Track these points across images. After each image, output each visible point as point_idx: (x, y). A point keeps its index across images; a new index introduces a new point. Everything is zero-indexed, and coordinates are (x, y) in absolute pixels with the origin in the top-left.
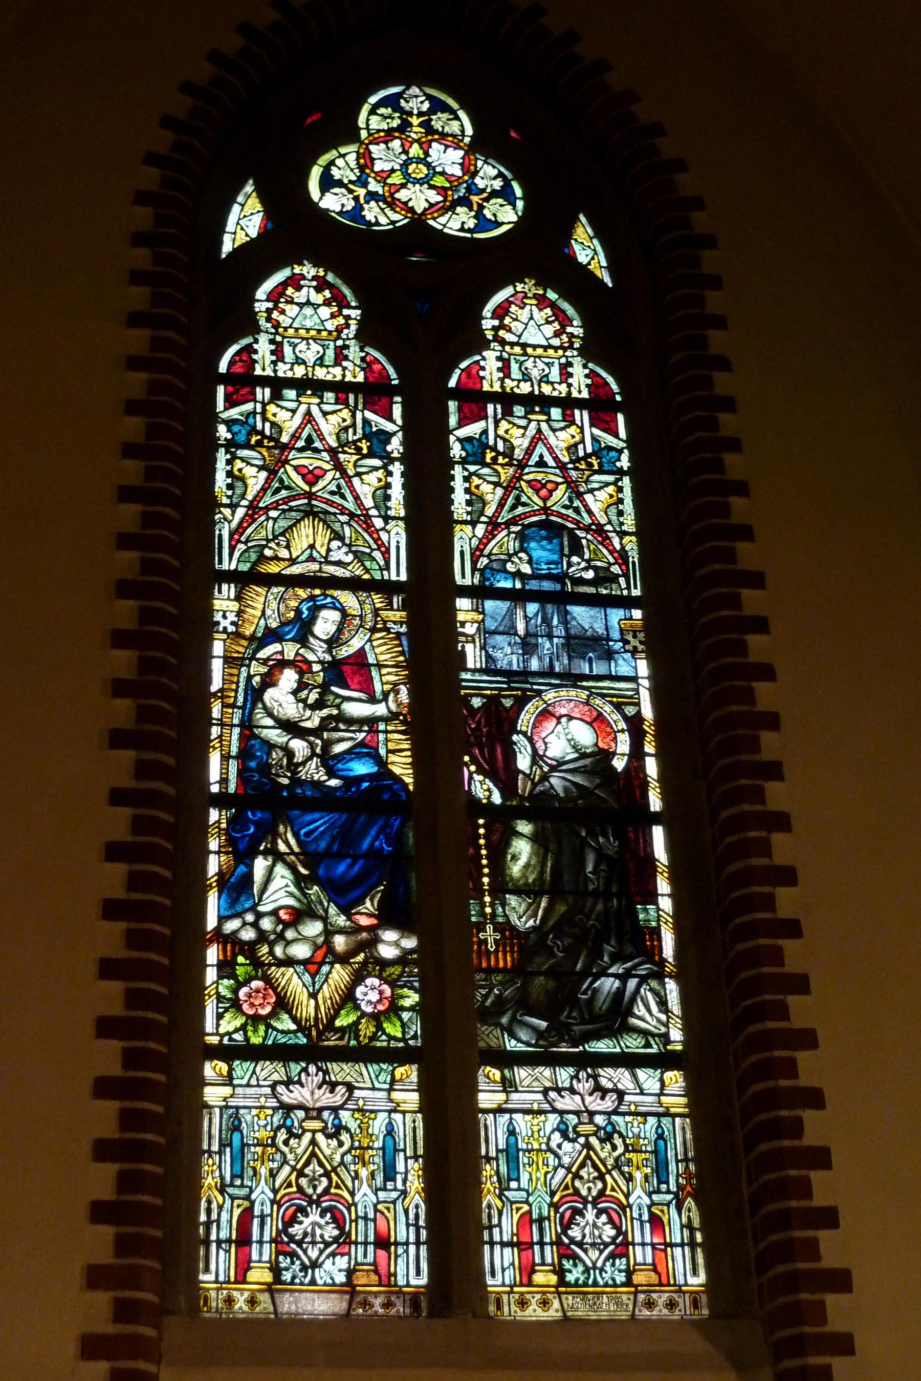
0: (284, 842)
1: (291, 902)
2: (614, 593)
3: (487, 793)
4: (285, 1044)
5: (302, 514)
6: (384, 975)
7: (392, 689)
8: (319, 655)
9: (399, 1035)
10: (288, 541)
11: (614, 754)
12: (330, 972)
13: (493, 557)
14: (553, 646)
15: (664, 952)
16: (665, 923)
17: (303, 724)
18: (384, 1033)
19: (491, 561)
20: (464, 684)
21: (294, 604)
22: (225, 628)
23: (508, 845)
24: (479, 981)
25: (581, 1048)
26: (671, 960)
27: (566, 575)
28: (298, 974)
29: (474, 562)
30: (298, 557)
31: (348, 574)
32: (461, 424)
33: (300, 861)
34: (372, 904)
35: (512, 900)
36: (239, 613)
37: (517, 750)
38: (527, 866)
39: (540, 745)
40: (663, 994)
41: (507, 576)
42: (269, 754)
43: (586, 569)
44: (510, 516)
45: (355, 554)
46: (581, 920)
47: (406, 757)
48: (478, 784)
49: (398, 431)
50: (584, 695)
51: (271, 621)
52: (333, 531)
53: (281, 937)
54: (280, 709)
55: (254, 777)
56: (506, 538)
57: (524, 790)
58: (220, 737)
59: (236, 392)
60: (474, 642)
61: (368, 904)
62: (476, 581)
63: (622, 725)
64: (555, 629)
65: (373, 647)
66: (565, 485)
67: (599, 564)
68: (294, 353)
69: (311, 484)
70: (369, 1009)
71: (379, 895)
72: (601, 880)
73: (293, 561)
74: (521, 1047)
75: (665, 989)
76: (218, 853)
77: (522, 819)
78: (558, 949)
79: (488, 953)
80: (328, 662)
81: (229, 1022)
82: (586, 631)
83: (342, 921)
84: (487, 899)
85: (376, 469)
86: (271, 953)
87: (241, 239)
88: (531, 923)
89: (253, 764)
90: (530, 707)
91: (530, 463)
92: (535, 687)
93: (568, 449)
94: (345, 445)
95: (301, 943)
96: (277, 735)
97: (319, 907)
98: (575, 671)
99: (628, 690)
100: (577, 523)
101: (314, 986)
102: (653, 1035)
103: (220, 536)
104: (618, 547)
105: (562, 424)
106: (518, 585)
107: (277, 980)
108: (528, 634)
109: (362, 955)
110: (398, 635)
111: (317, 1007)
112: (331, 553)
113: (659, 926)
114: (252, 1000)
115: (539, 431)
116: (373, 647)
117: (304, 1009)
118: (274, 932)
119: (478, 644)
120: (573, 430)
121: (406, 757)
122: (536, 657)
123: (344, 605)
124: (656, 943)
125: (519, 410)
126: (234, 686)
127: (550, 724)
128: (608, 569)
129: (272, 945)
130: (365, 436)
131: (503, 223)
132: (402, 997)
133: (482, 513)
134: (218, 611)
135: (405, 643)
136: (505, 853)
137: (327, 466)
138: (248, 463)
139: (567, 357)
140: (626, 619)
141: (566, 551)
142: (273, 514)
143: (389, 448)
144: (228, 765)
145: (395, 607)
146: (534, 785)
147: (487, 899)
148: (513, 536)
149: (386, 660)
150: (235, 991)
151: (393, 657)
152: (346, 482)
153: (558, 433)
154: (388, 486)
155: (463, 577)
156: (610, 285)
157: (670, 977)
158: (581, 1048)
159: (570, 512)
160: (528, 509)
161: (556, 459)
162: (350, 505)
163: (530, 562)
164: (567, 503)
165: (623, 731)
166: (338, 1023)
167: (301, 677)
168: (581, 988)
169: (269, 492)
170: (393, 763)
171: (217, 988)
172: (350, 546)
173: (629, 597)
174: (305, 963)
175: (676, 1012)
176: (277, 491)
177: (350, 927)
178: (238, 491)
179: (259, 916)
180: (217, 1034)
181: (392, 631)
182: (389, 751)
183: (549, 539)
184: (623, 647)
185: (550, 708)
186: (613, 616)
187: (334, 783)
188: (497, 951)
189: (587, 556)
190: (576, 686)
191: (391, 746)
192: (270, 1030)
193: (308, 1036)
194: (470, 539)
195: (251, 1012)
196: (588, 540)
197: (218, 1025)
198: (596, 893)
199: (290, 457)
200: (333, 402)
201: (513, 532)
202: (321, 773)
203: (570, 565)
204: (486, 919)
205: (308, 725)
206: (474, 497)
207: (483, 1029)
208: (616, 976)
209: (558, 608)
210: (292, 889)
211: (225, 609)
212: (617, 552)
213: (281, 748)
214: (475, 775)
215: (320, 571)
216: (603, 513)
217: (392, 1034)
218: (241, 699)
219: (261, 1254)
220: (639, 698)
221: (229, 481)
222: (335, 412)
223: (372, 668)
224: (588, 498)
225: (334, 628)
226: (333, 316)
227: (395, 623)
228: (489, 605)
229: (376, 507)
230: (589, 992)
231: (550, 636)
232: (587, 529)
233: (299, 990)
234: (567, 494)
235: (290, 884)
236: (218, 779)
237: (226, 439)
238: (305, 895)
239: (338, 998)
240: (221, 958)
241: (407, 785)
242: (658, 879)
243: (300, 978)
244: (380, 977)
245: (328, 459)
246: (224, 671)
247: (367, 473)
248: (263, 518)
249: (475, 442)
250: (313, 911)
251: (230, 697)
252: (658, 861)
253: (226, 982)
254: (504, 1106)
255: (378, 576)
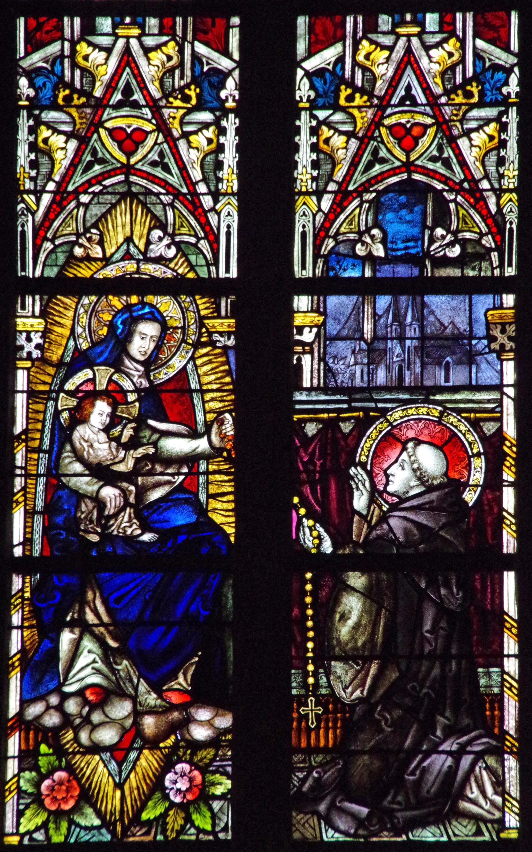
0: (92, 611)
1: (96, 679)
2: (483, 274)
3: (316, 541)
4: (88, 842)
5: (118, 196)
6: (196, 759)
7: (216, 419)
8: (135, 380)
9: (209, 828)
10: (101, 235)
11: (466, 485)
12: (138, 759)
13: (341, 238)
14: (404, 351)
15: (506, 723)
16: (510, 689)
17: (115, 468)
18: (193, 825)
19: (338, 243)
20: (298, 407)
21: (107, 317)
22: (29, 354)
23: (337, 602)
24: (296, 763)
25: (404, 837)
26: (512, 732)
27: (427, 254)
28: (104, 762)
29: (317, 247)
30: (112, 255)
31: (169, 274)
33: (109, 632)
34: (186, 679)
35: (338, 667)
36: (45, 333)
37: (354, 486)
38: (357, 626)
39: (380, 480)
40: (500, 772)
41: (356, 262)
42: (78, 507)
43: (451, 244)
44: (364, 179)
45: (178, 245)
46: (413, 688)
47: (228, 502)
48: (307, 531)
49: (234, 69)
50: (436, 411)
51: (81, 340)
52: (154, 217)
53: (87, 720)
54: (91, 451)
55: (61, 534)
56: (358, 210)
57: (359, 536)
58: (24, 489)
59: (40, 27)
60: (311, 352)
61: (181, 679)
62: (318, 272)
63: (478, 447)
64: (408, 328)
65: (196, 367)
66: (434, 129)
67: (468, 235)
69: (129, 154)
70: (178, 800)
71: (193, 668)
72: (440, 640)
73: (106, 261)
74: (340, 837)
75: (503, 767)
76: (21, 628)
77: (354, 570)
78: (385, 724)
79: (309, 730)
80: (145, 389)
81: (30, 820)
82: (446, 328)
83: (152, 699)
84: (311, 668)
85: (206, 125)
86: (76, 739)
88: (358, 693)
89: (59, 519)
90: (372, 431)
91: (392, 102)
92: (380, 405)
93: (443, 74)
94: (170, 95)
95: (107, 726)
96: (87, 483)
97: (128, 684)
98: (428, 383)
99: (489, 401)
100: (444, 180)
101: (120, 776)
102: (486, 821)
103: (23, 233)
104: (493, 209)
105: (438, 38)
106: (368, 273)
107: (82, 769)
108: (375, 337)
109: (173, 738)
110: (225, 348)
111: (123, 798)
112: (152, 247)
113: (502, 692)
114: (55, 794)
115: (409, 51)
116: (196, 367)
117: (110, 802)
118: (80, 715)
119: (316, 355)
120: (451, 45)
121: (228, 502)
122: (383, 366)
123: (165, 314)
124: (496, 713)
126: (39, 426)
127: (394, 453)
128: (478, 242)
129: (76, 730)
130: (195, 80)
132: (214, 784)
133: (330, 178)
134: (21, 332)
135: (232, 359)
136: (334, 612)
137: (148, 127)
138: (56, 131)
140: (494, 308)
141: (429, 222)
142: (84, 198)
143: (223, 94)
144: (33, 522)
145: (223, 313)
146: (371, 528)
147: (311, 668)
148: (366, 205)
149: (210, 383)
150: (37, 785)
151: (218, 379)
152: (170, 148)
154: (221, 148)
155: (304, 267)
157: (511, 753)
158: (404, 837)
159: (438, 167)
160: (386, 167)
161: (426, 89)
162: (175, 180)
163: (384, 241)
164: (435, 153)
165: (478, 455)
166: (145, 816)
167: (114, 409)
168: (408, 767)
169: (80, 169)
170: (214, 510)
171: (18, 782)
173: (502, 276)
174: (111, 749)
175: (513, 794)
176: (89, 166)
177: (161, 706)
178: (44, 170)
179: (65, 697)
180: (17, 834)
181: (218, 344)
182: (210, 496)
183: (409, 207)
184: (488, 346)
185: (396, 431)
186: (480, 305)
187: (147, 537)
188: (318, 727)
189: (454, 227)
190: (427, 401)
191: (213, 489)
192: (73, 827)
193: (113, 833)
194: (314, 216)
195: (53, 808)
196: (457, 204)
197: (18, 824)
198: (432, 656)
199: (105, 117)
200: (156, 31)
201: (367, 201)
202: (135, 526)
203: (432, 241)
204: (308, 690)
205: (121, 468)
206: (322, 156)
207: (299, 817)
208: (449, 753)
209: (414, 299)
210: (99, 665)
211: (30, 329)
212: (493, 216)
213: (90, 498)
214: (304, 520)
215: (138, 271)
216: (478, 164)
217: (201, 827)
218: (47, 440)
220: (501, 412)
221: (33, 156)
222: (158, 47)
223: (194, 395)
224: (463, 143)
225: (152, 345)
227: (221, 334)
228: (333, 301)
229: (205, 180)
230: (418, 772)
231: (402, 339)
232: (457, 188)
233: (105, 780)
234: (437, 140)
235: (97, 659)
236: (22, 540)
237: (28, 98)
238: (113, 671)
239: (145, 788)
240: (23, 747)
241: (228, 536)
242: (506, 635)
243: (105, 766)
244: (190, 762)
245: (150, 116)
246: (28, 408)
247: (195, 133)
248: (73, 204)
249: (327, 75)
250: (122, 689)
251: (34, 439)
252: (507, 615)
253: (27, 775)
255: (203, 273)
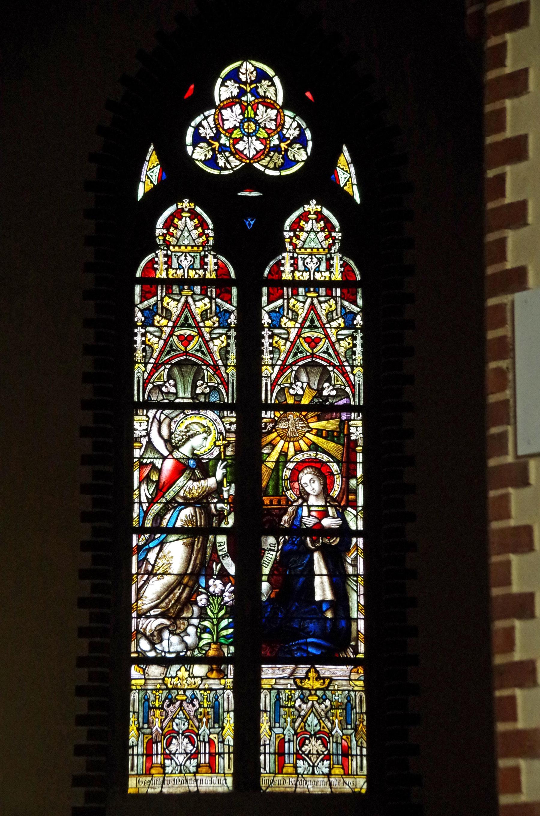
68: (178, 262)
125: (301, 290)
139: (331, 254)
153: (322, 305)
226: (200, 236)
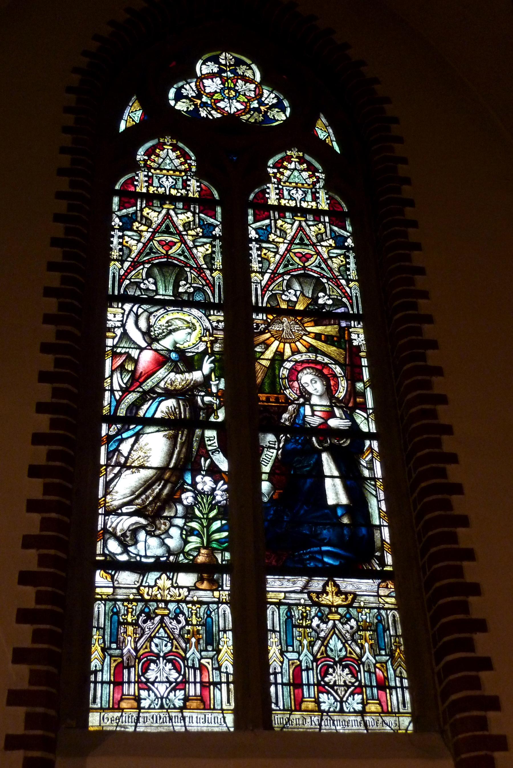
32: (255, 221)
87: (131, 124)
131: (278, 120)
139: (316, 189)
153: (311, 227)
156: (339, 152)
172: (191, 284)
219: (129, 690)
226: (181, 164)
254: (283, 601)
